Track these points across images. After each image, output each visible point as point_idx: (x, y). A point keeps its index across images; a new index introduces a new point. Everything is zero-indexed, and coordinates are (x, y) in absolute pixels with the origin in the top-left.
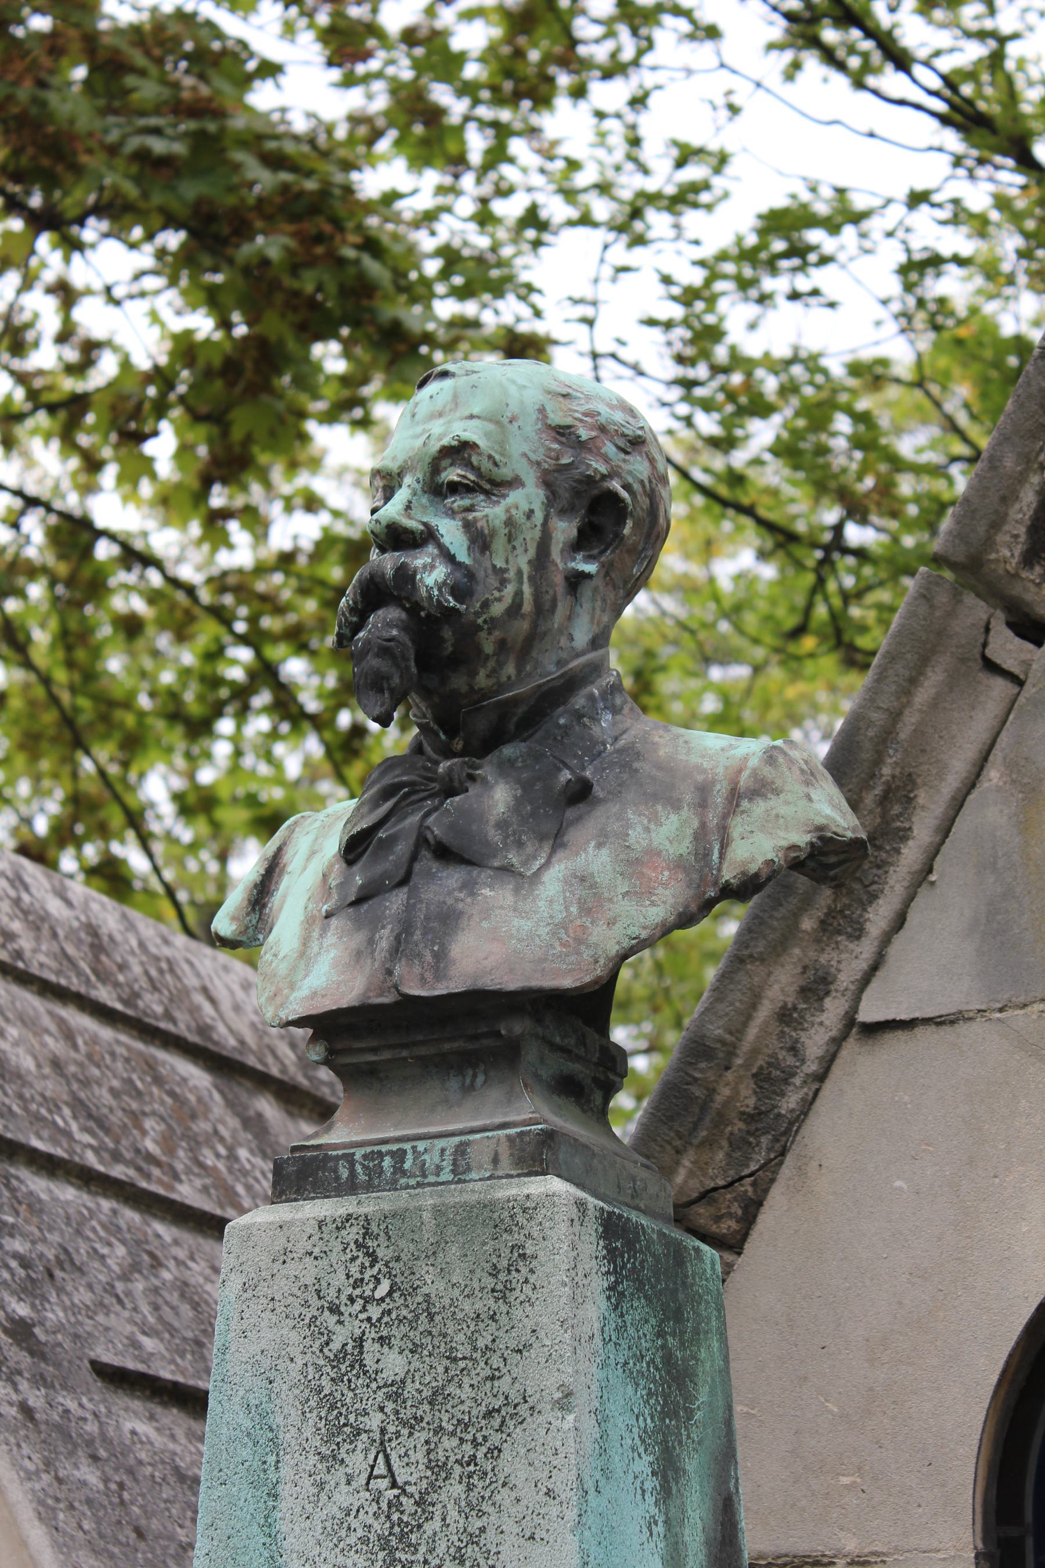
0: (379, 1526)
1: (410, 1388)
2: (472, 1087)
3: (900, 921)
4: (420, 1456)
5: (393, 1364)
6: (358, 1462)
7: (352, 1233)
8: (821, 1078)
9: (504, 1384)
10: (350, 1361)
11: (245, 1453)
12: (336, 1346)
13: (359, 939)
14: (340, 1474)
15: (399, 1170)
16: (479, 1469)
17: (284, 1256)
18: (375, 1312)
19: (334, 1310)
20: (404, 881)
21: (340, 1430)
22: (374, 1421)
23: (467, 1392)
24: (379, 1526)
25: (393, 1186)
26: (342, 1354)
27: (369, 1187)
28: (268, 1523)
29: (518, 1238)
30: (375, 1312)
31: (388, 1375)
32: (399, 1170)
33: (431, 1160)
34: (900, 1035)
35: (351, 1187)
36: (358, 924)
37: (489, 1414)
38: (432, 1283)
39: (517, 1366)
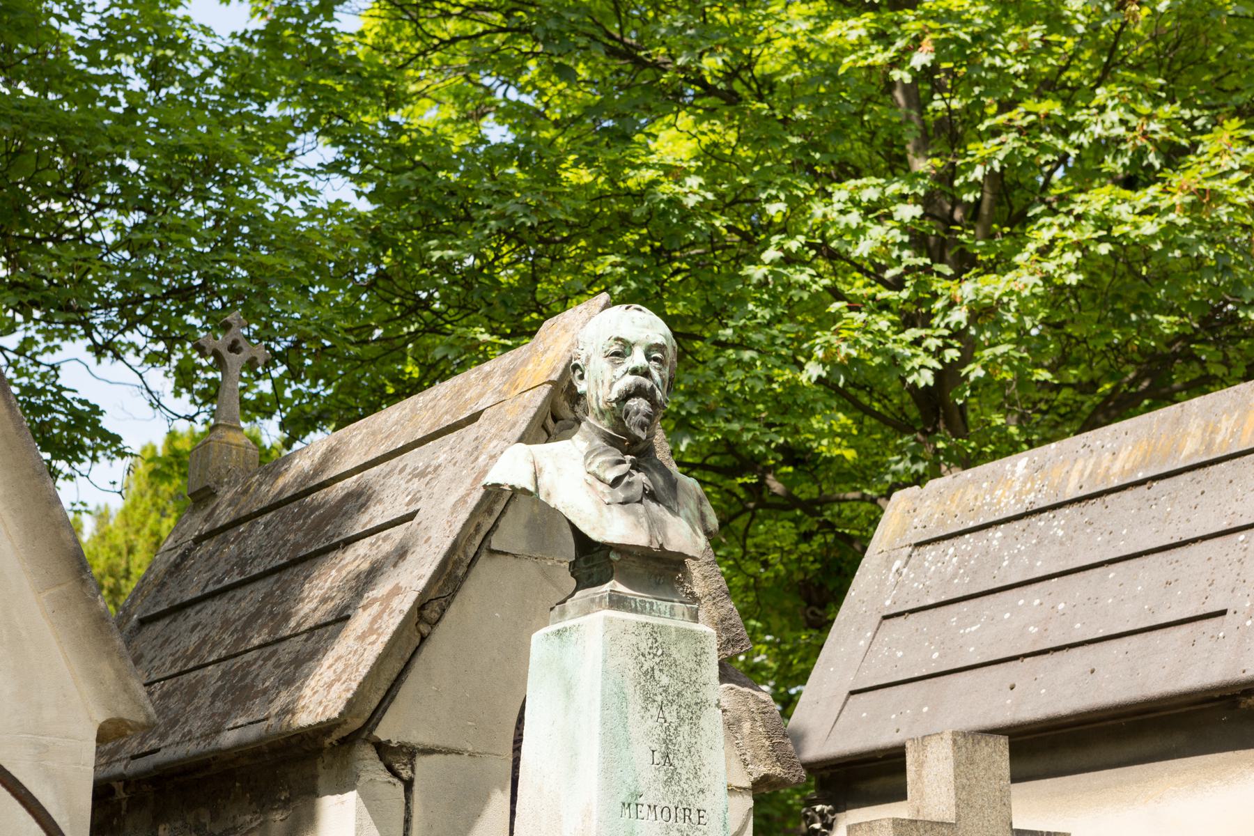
0: (663, 735)
1: (671, 690)
2: (658, 584)
3: (503, 512)
4: (675, 713)
5: (665, 680)
6: (654, 711)
7: (648, 629)
8: (469, 566)
9: (700, 695)
10: (650, 674)
11: (616, 700)
12: (645, 668)
13: (632, 519)
14: (648, 714)
15: (651, 609)
16: (694, 720)
17: (625, 632)
18: (657, 659)
19: (643, 655)
20: (640, 502)
21: (648, 698)
22: (659, 698)
23: (689, 695)
24: (663, 735)
25: (650, 614)
26: (646, 673)
27: (642, 613)
28: (624, 727)
29: (702, 645)
30: (657, 659)
31: (662, 683)
32: (651, 609)
33: (662, 608)
34: (502, 557)
35: (635, 611)
36: (629, 512)
37: (696, 704)
38: (676, 655)
39: (704, 689)
